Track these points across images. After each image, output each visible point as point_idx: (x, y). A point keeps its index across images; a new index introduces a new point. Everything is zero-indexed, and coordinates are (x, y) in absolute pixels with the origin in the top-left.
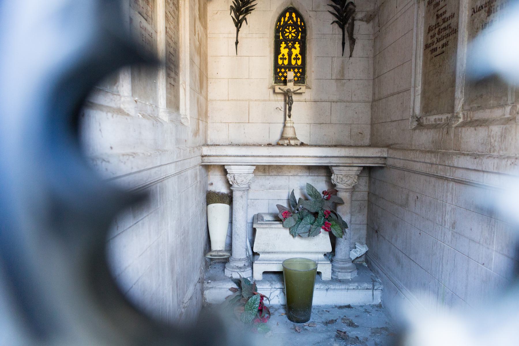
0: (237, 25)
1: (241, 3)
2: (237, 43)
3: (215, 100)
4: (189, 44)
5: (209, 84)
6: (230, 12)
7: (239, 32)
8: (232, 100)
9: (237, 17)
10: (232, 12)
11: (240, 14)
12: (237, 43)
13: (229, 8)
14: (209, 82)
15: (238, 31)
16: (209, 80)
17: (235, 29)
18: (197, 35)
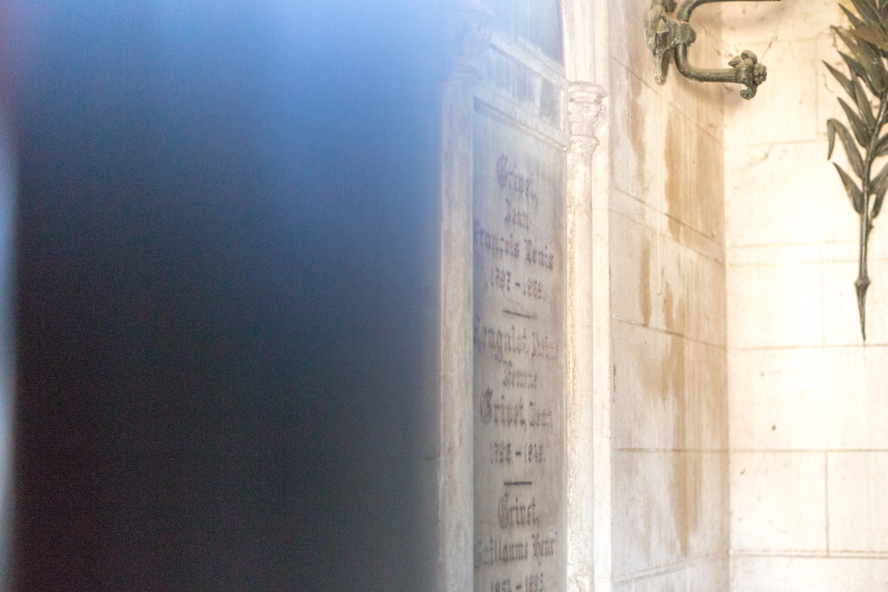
0: (859, 206)
1: (875, 101)
2: (862, 288)
3: (766, 553)
4: (607, 395)
5: (735, 477)
6: (826, 144)
7: (873, 235)
8: (847, 554)
9: (863, 170)
10: (839, 144)
11: (874, 154)
12: (862, 288)
13: (824, 128)
14: (735, 468)
15: (868, 228)
16: (733, 457)
17: (855, 218)
18: (657, 319)
